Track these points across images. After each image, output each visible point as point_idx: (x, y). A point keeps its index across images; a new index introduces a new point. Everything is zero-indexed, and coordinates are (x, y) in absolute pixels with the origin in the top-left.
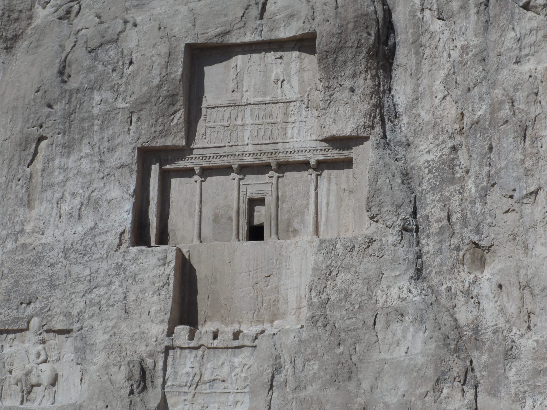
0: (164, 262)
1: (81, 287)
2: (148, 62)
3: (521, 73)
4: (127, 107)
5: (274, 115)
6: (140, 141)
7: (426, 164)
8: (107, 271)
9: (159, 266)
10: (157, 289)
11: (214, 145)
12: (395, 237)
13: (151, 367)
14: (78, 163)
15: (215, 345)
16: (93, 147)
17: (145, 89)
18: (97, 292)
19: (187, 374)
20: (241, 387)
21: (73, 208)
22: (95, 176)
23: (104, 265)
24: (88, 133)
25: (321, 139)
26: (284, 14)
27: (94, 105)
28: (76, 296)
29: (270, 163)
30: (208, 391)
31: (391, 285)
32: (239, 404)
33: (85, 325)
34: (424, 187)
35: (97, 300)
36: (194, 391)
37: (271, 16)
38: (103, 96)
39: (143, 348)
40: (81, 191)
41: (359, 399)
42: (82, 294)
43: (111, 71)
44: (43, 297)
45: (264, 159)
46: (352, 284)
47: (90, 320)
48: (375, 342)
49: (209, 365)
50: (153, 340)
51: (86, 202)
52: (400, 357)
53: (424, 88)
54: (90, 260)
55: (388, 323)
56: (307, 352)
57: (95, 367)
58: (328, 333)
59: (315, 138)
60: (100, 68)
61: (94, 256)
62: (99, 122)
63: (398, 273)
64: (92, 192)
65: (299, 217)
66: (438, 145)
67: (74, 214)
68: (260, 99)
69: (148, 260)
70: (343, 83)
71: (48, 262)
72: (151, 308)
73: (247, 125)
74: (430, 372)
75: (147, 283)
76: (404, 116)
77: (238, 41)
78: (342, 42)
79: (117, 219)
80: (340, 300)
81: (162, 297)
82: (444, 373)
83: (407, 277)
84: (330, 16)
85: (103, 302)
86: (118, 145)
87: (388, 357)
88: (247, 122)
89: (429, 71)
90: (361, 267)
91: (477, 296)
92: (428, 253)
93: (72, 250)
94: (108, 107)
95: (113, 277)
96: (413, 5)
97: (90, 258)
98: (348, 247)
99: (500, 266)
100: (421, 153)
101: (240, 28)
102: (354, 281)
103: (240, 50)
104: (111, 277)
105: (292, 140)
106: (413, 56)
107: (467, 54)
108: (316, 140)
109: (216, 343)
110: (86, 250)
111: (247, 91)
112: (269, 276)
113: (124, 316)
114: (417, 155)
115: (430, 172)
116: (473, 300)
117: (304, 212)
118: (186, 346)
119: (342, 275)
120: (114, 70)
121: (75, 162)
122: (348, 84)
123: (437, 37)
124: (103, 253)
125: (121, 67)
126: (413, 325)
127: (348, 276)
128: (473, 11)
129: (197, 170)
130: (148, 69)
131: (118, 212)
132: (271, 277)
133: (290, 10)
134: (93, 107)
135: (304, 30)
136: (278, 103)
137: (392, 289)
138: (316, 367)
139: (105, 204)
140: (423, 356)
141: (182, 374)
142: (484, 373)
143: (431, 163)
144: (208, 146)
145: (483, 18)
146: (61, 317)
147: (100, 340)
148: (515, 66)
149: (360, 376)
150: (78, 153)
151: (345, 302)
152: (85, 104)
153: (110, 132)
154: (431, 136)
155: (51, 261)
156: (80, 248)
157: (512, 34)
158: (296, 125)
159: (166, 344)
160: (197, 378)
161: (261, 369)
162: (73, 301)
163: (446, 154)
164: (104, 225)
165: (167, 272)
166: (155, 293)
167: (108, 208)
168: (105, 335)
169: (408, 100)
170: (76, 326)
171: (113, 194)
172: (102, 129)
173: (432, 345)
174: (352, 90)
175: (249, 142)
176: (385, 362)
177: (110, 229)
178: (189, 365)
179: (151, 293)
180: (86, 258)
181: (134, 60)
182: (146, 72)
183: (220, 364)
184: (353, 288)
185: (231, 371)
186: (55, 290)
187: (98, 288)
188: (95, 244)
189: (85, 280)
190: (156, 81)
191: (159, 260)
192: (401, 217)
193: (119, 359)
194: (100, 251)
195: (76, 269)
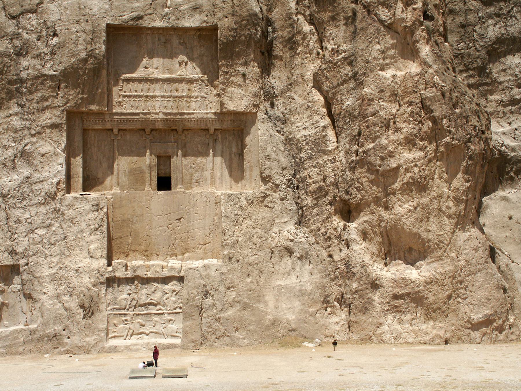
0: (97, 207)
1: (22, 228)
2: (74, 37)
3: (385, 78)
4: (55, 75)
5: (180, 90)
6: (68, 105)
7: (304, 138)
8: (46, 214)
9: (93, 211)
10: (93, 230)
11: (131, 111)
12: (283, 193)
13: (96, 296)
14: (8, 120)
15: (149, 276)
16: (22, 106)
17: (73, 60)
18: (38, 232)
19: (126, 299)
20: (172, 308)
21: (6, 159)
22: (26, 132)
23: (43, 209)
24: (16, 94)
25: (219, 111)
26: (187, 6)
27: (22, 69)
28: (19, 236)
30: (145, 312)
31: (281, 229)
32: (172, 322)
33: (30, 260)
34: (302, 156)
35: (39, 239)
36: (132, 313)
37: (177, 7)
38: (30, 62)
39: (88, 279)
40: (13, 144)
41: (268, 317)
42: (25, 234)
43: (35, 39)
46: (254, 228)
47: (34, 256)
48: (273, 272)
49: (144, 291)
50: (95, 272)
51: (19, 154)
52: (292, 283)
53: (297, 77)
54: (29, 205)
55: (281, 257)
56: (227, 282)
57: (45, 296)
58: (240, 266)
60: (25, 35)
61: (32, 202)
62: (28, 85)
63: (286, 220)
64: (25, 146)
65: (200, 172)
66: (313, 124)
67: (7, 164)
68: (167, 76)
69: (83, 206)
70: (237, 69)
72: (89, 245)
73: (158, 97)
74: (317, 295)
75: (83, 226)
76: (279, 97)
77: (150, 26)
78: (238, 36)
79: (51, 170)
80: (246, 242)
81: (98, 237)
82: (328, 296)
83: (293, 222)
84: (228, 14)
85: (45, 241)
86: (47, 106)
87: (283, 284)
88: (157, 94)
89: (302, 64)
90: (259, 215)
91: (347, 240)
92: (307, 205)
93: (10, 196)
94: (36, 73)
95: (52, 220)
96: (289, 9)
97: (29, 203)
98: (249, 200)
99: (365, 218)
101: (150, 14)
102: (255, 226)
103: (149, 32)
104: (50, 220)
105: (196, 111)
107: (338, 56)
108: (215, 113)
109: (150, 274)
110: (24, 196)
111: (156, 68)
112: (180, 219)
113: (67, 253)
114: (294, 130)
116: (343, 242)
117: (203, 168)
118: (124, 277)
119: (246, 221)
120: (38, 40)
121: (4, 118)
122: (241, 69)
123: (309, 37)
124: (40, 199)
125: (45, 38)
127: (251, 222)
128: (343, 22)
129: (115, 131)
130: (74, 43)
131: (51, 164)
132: (182, 219)
133: (192, 3)
134: (21, 71)
135: (207, 23)
137: (282, 232)
138: (234, 293)
139: (39, 157)
140: (311, 284)
141: (122, 299)
142: (355, 296)
143: (308, 137)
144: (125, 111)
145: (352, 28)
146: (6, 254)
147: (47, 274)
148: (380, 73)
149: (267, 298)
150: (7, 110)
151: (250, 242)
152: (11, 68)
153: (39, 95)
154: (305, 116)
156: (18, 194)
157: (378, 47)
158: (199, 99)
159: (107, 275)
160: (134, 302)
161: (192, 295)
162: (16, 241)
163: (320, 132)
164: (39, 175)
165: (100, 217)
166: (91, 233)
167: (42, 160)
168: (51, 270)
169: (283, 85)
170: (22, 262)
171: (46, 148)
172: (31, 92)
173: (317, 277)
174: (244, 75)
176: (281, 287)
177: (46, 179)
178: (126, 292)
179: (88, 233)
180: (24, 203)
181: (58, 32)
182: (73, 46)
183: (153, 289)
184: (254, 231)
185: (163, 296)
187: (39, 229)
188: (32, 191)
189: (26, 222)
190: (83, 55)
191: (93, 206)
192: (286, 178)
193: (68, 289)
194: (37, 198)
195: (17, 213)
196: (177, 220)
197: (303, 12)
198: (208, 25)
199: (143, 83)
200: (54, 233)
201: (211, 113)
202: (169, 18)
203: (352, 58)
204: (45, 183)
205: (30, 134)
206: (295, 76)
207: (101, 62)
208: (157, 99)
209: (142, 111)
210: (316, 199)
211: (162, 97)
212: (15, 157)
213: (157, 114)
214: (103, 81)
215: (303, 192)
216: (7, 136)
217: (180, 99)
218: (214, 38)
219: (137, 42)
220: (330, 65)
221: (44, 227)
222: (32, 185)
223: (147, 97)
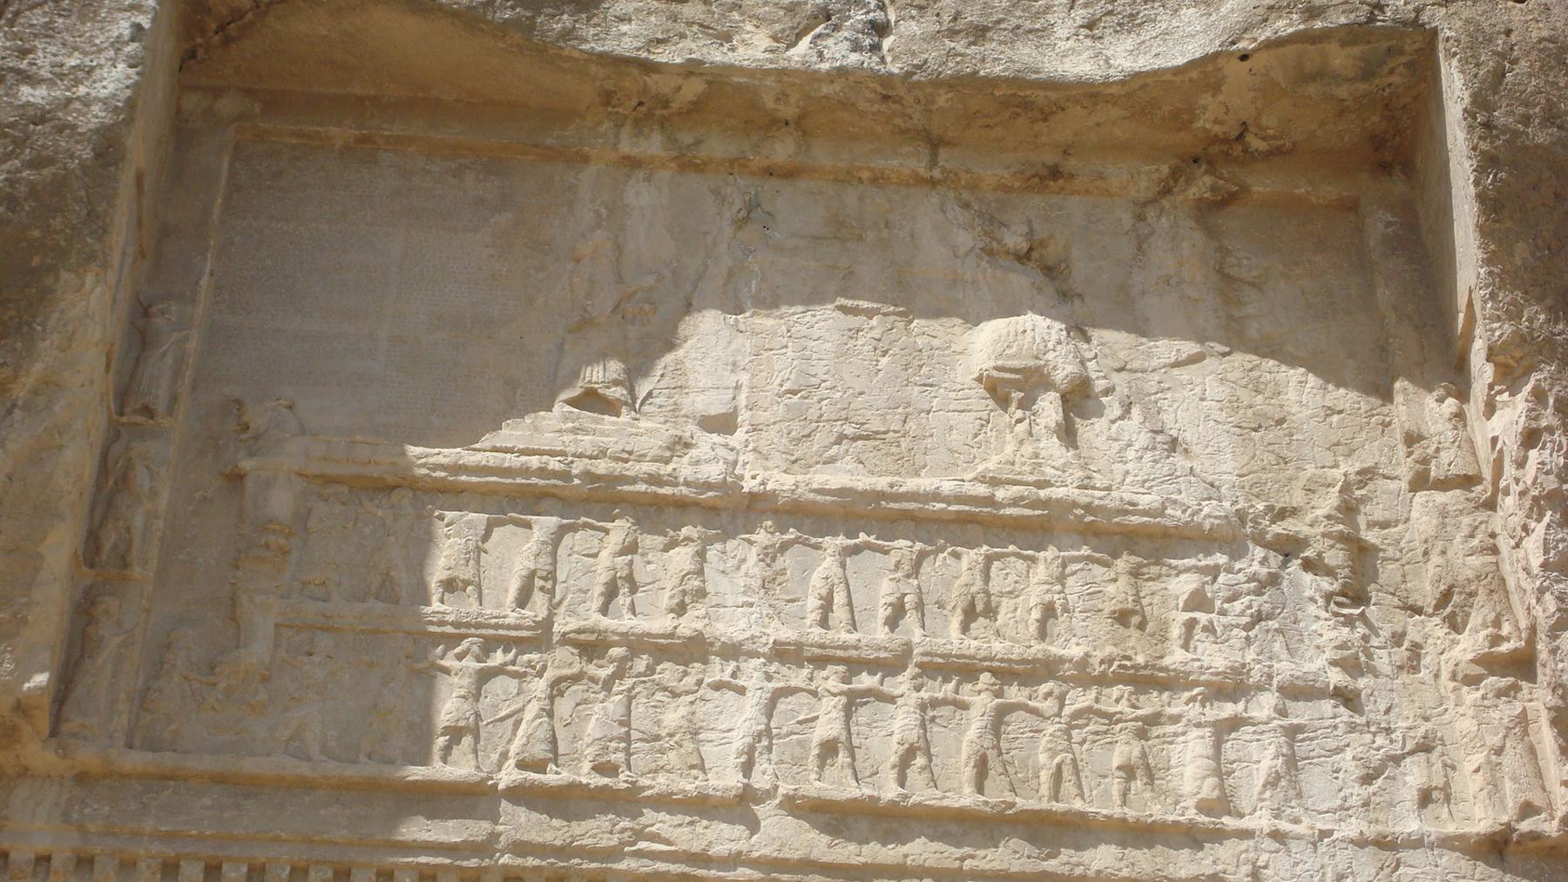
59: (1481, 820)
73: (733, 651)
88: (731, 626)
103: (653, 145)
105: (1229, 822)
111: (723, 424)
175: (760, 781)
198: (1318, 24)
199: (546, 524)
201: (1447, 843)
202: (881, 29)
207: (60, 185)
208: (719, 670)
209: (508, 776)
211: (785, 654)
214: (50, 386)
217: (1015, 694)
218: (1379, 224)
219: (504, 219)
223: (591, 646)
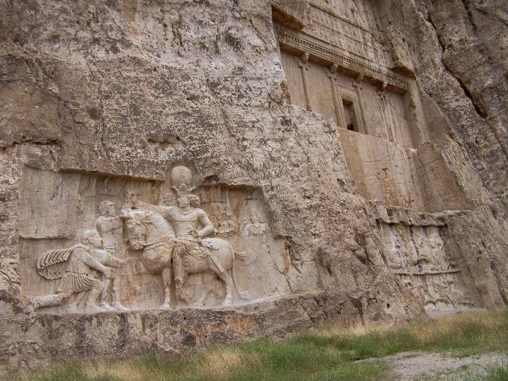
9: (327, 132)
11: (322, 39)
25: (392, 68)
29: (359, 73)
44: (191, 138)
45: (356, 68)
53: (428, 61)
64: (229, 29)
71: (186, 93)
93: (221, 86)
100: (448, 101)
106: (414, 38)
115: (465, 113)
126: (505, 219)
136: (358, 27)
143: (464, 108)
155: (192, 92)
170: (263, 183)
186: (211, 131)
194: (259, 98)
196: (383, 169)
197: (422, 9)
200: (293, 150)
203: (482, 47)
204: (263, 82)
205: (234, 17)
206: (426, 60)
210: (490, 162)
212: (217, 39)
213: (345, 50)
215: (475, 157)
216: (201, 11)
220: (463, 51)
221: (276, 140)
222: (247, 80)
